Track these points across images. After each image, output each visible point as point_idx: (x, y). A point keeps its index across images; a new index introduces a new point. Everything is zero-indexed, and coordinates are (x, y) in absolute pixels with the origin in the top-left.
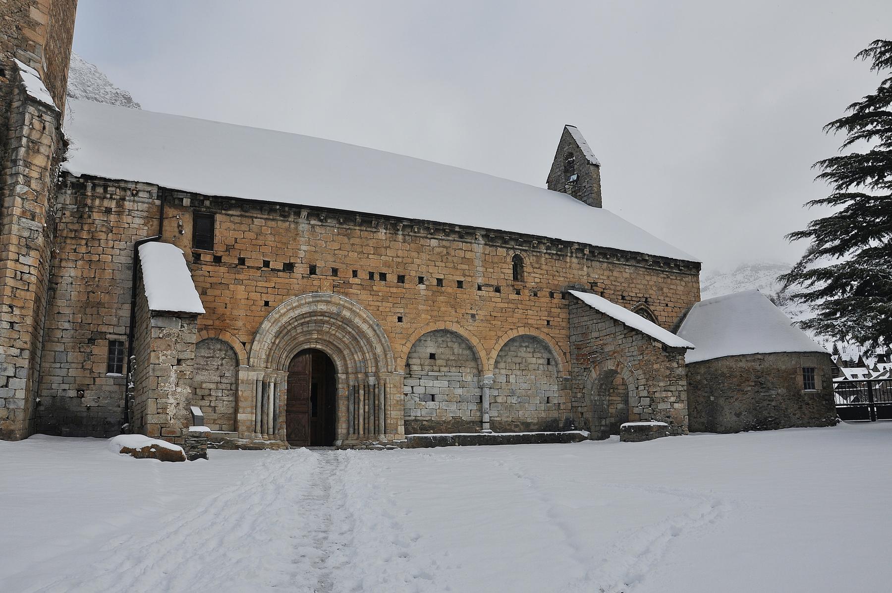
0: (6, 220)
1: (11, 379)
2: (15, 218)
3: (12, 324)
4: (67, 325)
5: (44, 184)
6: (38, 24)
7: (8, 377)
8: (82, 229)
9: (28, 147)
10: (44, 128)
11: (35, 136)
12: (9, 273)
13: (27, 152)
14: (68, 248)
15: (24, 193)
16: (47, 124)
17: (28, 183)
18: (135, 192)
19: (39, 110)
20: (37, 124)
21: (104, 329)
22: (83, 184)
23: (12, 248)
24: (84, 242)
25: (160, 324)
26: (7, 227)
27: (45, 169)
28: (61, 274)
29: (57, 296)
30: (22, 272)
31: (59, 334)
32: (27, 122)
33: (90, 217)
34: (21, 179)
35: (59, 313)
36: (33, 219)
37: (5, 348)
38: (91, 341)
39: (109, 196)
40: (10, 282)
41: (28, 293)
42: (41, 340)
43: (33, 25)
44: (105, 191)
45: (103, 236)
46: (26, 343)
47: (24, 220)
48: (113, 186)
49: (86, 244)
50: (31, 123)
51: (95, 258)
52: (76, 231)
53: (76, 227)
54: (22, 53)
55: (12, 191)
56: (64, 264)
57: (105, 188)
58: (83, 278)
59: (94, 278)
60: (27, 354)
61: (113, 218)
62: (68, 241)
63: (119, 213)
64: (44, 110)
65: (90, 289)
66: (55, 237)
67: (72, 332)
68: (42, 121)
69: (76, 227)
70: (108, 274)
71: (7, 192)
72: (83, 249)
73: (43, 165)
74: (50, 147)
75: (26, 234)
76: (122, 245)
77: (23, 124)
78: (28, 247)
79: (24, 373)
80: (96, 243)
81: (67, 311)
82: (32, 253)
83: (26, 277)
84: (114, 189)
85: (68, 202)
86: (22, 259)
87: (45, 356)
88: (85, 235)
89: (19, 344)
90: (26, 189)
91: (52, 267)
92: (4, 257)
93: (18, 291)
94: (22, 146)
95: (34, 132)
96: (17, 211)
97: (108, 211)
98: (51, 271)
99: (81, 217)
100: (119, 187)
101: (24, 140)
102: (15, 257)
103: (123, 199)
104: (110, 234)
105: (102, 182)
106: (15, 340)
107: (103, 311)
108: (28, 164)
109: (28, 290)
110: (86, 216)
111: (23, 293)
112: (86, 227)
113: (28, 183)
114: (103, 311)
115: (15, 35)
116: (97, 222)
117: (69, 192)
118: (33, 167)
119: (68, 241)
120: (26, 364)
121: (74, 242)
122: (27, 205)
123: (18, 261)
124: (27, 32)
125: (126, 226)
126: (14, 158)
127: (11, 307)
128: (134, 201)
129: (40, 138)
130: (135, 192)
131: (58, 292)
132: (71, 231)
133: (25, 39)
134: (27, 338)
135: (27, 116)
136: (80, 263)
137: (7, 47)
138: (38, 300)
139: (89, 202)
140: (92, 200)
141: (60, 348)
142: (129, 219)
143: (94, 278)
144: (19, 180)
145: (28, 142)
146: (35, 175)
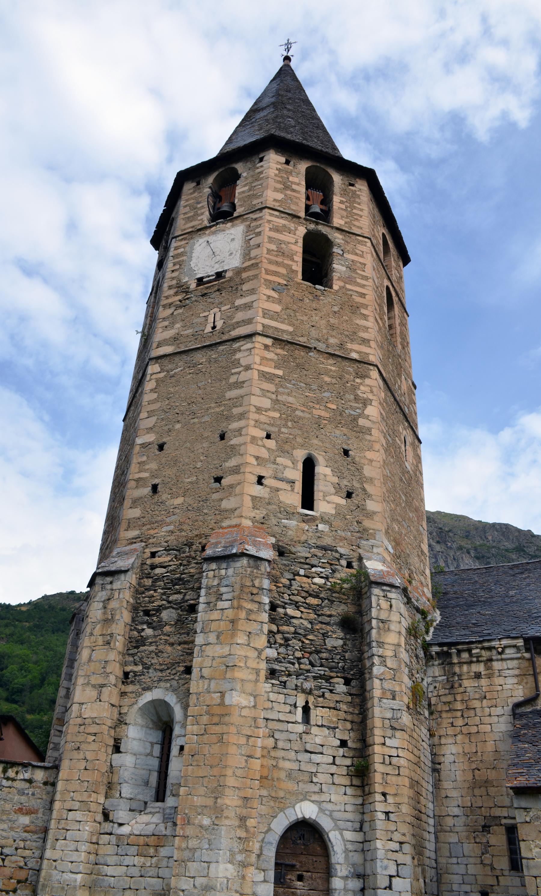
0: (369, 705)
1: (393, 879)
2: (376, 700)
3: (387, 813)
4: (457, 811)
5: (400, 661)
6: (374, 513)
7: (391, 877)
8: (455, 700)
9: (379, 628)
10: (391, 606)
11: (383, 616)
12: (377, 759)
13: (379, 633)
14: (445, 723)
15: (382, 674)
16: (393, 602)
17: (384, 663)
18: (500, 650)
19: (384, 591)
20: (384, 604)
21: (497, 812)
22: (447, 652)
23: (377, 732)
24: (459, 714)
25: (524, 804)
26: (370, 710)
27: (399, 645)
28: (442, 753)
29: (442, 778)
30: (390, 756)
31: (450, 821)
32: (374, 604)
33: (460, 686)
34: (376, 660)
35: (447, 797)
36: (394, 698)
37: (383, 842)
38: (486, 828)
39: (475, 659)
40: (379, 767)
41: (400, 778)
42: (432, 830)
43: (370, 515)
44: (471, 655)
45: (476, 704)
46: (404, 835)
47: (385, 701)
48: (477, 648)
49: (462, 716)
50: (378, 605)
51: (474, 729)
52: (449, 703)
53: (449, 698)
54: (365, 542)
55: (370, 673)
56: (443, 741)
57: (469, 651)
58: (465, 754)
59: (477, 752)
60: (407, 848)
61: (484, 682)
62: (444, 715)
63: (490, 677)
64: (388, 588)
65: (474, 766)
66: (431, 713)
67: (464, 818)
68: (389, 600)
69: (449, 698)
70: (490, 747)
71: (367, 676)
72: (460, 722)
73: (396, 642)
74: (400, 622)
75: (389, 715)
76: (499, 711)
77: (371, 607)
78: (393, 728)
79: (405, 871)
80: (472, 713)
81: (454, 794)
82: (398, 734)
83: (395, 760)
84: (478, 651)
85: (437, 674)
86: (388, 742)
87: (440, 849)
88: (459, 706)
89: (397, 837)
90: (382, 669)
91: (432, 746)
92: (371, 743)
93: (389, 777)
94: (372, 628)
95: (382, 612)
96: (377, 693)
97: (478, 676)
98: (432, 751)
99: (452, 687)
100: (483, 648)
101: (374, 622)
102: (382, 740)
103: (491, 660)
104: (485, 701)
105: (465, 647)
106: (392, 832)
107: (492, 791)
108: (381, 644)
109: (399, 774)
110: (456, 685)
111: (394, 778)
112: (459, 697)
113: (384, 663)
114: (492, 791)
115: (357, 529)
116: (468, 690)
117: (436, 663)
118: (386, 646)
119: (444, 715)
120: (407, 859)
121: (449, 715)
122: (388, 685)
123: (384, 744)
124: (367, 523)
125: (500, 688)
126: (368, 641)
127: (384, 794)
128: (502, 660)
129: (389, 616)
130: (500, 650)
131: (442, 773)
132: (445, 703)
133: (365, 530)
134: (404, 828)
135: (374, 599)
136: (459, 737)
137: (352, 542)
138: (415, 784)
139: (457, 669)
140: (460, 667)
141: (453, 838)
142: (501, 680)
143: (477, 752)
144: (375, 661)
145: (378, 623)
146: (389, 653)
